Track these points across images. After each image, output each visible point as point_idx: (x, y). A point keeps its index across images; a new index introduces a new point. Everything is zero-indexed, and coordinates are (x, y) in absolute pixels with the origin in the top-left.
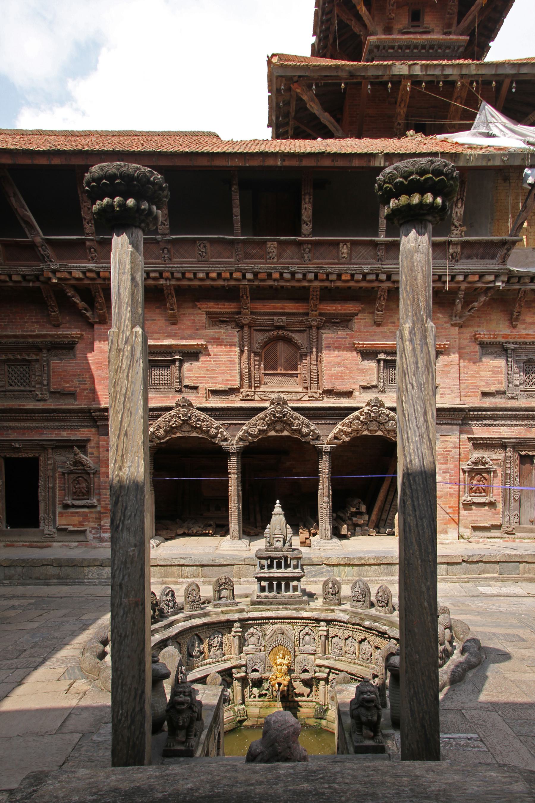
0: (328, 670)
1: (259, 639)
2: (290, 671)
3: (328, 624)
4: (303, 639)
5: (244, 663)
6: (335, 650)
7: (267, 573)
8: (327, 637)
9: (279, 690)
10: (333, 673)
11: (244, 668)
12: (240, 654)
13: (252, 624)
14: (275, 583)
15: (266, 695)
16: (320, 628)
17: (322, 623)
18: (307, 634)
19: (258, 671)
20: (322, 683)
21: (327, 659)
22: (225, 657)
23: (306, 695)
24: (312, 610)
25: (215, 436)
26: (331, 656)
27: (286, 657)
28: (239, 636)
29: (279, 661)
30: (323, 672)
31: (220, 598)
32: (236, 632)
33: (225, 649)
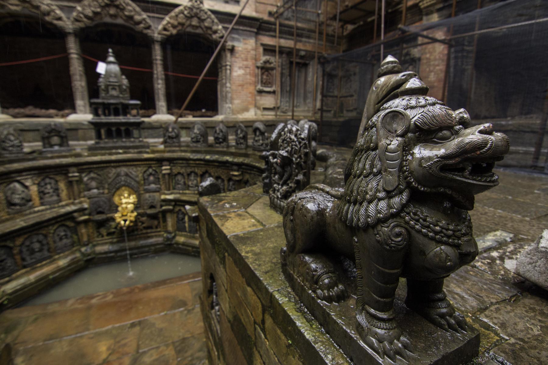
0: (173, 203)
3: (170, 163)
5: (86, 206)
7: (104, 119)
9: (124, 226)
11: (87, 212)
14: (114, 129)
16: (164, 168)
17: (164, 163)
18: (151, 174)
21: (171, 194)
23: (154, 227)
24: (153, 152)
25: (48, 14)
29: (124, 201)
30: (170, 205)
31: (52, 146)
33: (64, 194)
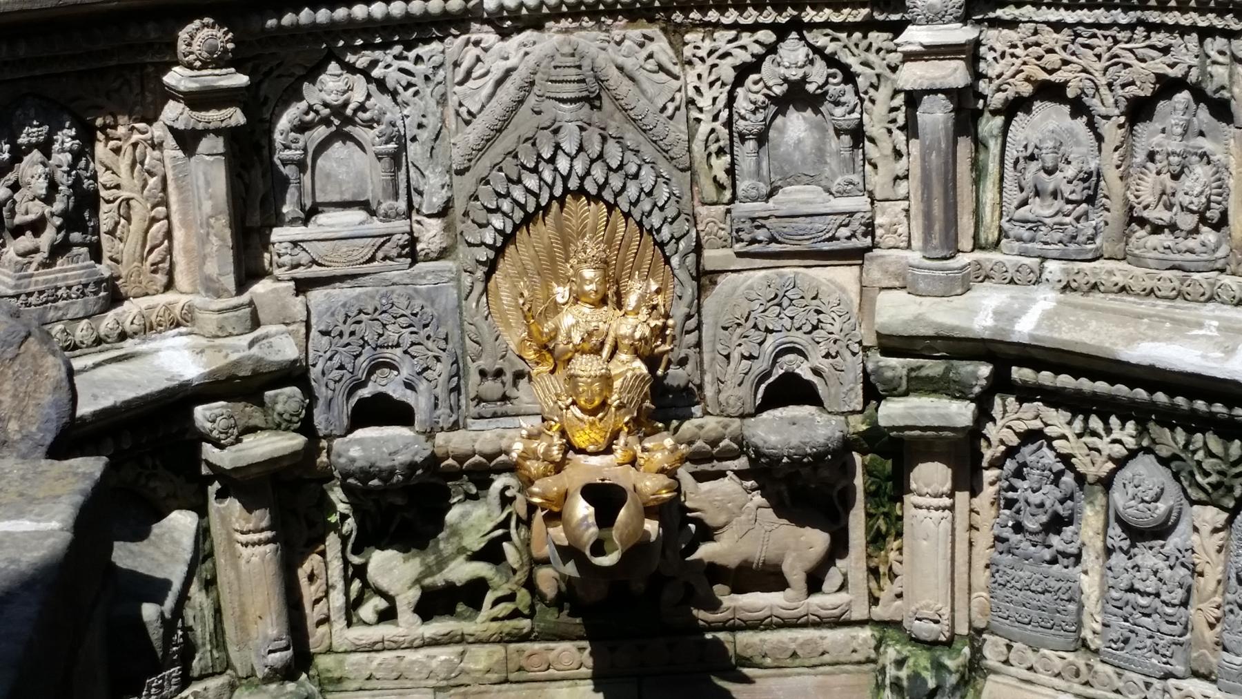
1: (396, 159)
2: (665, 403)
4: (762, 138)
5: (286, 349)
6: (1037, 208)
8: (966, 107)
10: (1026, 393)
11: (286, 398)
12: (241, 287)
13: (332, 30)
15: (474, 592)
18: (796, 96)
19: (400, 414)
20: (931, 476)
21: (965, 282)
22: (130, 311)
23: (795, 573)
26: (1006, 258)
27: (634, 292)
28: (230, 135)
32: (198, 100)
